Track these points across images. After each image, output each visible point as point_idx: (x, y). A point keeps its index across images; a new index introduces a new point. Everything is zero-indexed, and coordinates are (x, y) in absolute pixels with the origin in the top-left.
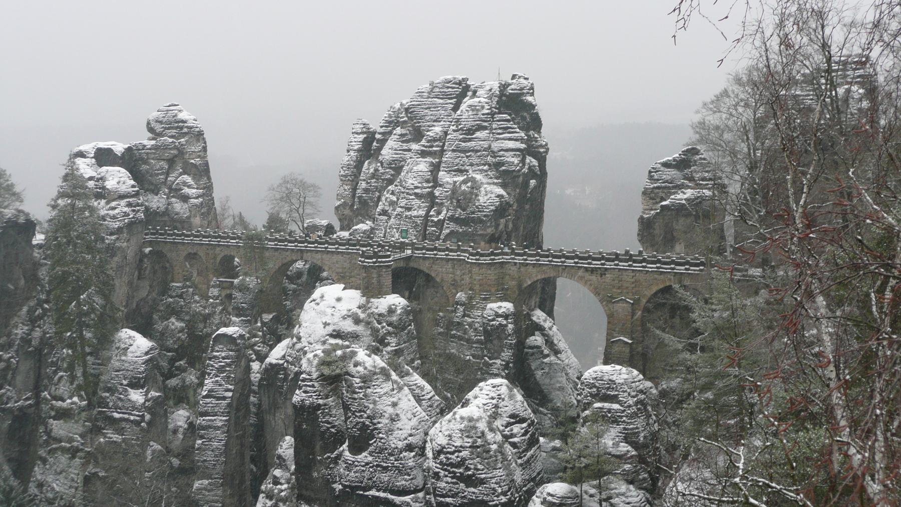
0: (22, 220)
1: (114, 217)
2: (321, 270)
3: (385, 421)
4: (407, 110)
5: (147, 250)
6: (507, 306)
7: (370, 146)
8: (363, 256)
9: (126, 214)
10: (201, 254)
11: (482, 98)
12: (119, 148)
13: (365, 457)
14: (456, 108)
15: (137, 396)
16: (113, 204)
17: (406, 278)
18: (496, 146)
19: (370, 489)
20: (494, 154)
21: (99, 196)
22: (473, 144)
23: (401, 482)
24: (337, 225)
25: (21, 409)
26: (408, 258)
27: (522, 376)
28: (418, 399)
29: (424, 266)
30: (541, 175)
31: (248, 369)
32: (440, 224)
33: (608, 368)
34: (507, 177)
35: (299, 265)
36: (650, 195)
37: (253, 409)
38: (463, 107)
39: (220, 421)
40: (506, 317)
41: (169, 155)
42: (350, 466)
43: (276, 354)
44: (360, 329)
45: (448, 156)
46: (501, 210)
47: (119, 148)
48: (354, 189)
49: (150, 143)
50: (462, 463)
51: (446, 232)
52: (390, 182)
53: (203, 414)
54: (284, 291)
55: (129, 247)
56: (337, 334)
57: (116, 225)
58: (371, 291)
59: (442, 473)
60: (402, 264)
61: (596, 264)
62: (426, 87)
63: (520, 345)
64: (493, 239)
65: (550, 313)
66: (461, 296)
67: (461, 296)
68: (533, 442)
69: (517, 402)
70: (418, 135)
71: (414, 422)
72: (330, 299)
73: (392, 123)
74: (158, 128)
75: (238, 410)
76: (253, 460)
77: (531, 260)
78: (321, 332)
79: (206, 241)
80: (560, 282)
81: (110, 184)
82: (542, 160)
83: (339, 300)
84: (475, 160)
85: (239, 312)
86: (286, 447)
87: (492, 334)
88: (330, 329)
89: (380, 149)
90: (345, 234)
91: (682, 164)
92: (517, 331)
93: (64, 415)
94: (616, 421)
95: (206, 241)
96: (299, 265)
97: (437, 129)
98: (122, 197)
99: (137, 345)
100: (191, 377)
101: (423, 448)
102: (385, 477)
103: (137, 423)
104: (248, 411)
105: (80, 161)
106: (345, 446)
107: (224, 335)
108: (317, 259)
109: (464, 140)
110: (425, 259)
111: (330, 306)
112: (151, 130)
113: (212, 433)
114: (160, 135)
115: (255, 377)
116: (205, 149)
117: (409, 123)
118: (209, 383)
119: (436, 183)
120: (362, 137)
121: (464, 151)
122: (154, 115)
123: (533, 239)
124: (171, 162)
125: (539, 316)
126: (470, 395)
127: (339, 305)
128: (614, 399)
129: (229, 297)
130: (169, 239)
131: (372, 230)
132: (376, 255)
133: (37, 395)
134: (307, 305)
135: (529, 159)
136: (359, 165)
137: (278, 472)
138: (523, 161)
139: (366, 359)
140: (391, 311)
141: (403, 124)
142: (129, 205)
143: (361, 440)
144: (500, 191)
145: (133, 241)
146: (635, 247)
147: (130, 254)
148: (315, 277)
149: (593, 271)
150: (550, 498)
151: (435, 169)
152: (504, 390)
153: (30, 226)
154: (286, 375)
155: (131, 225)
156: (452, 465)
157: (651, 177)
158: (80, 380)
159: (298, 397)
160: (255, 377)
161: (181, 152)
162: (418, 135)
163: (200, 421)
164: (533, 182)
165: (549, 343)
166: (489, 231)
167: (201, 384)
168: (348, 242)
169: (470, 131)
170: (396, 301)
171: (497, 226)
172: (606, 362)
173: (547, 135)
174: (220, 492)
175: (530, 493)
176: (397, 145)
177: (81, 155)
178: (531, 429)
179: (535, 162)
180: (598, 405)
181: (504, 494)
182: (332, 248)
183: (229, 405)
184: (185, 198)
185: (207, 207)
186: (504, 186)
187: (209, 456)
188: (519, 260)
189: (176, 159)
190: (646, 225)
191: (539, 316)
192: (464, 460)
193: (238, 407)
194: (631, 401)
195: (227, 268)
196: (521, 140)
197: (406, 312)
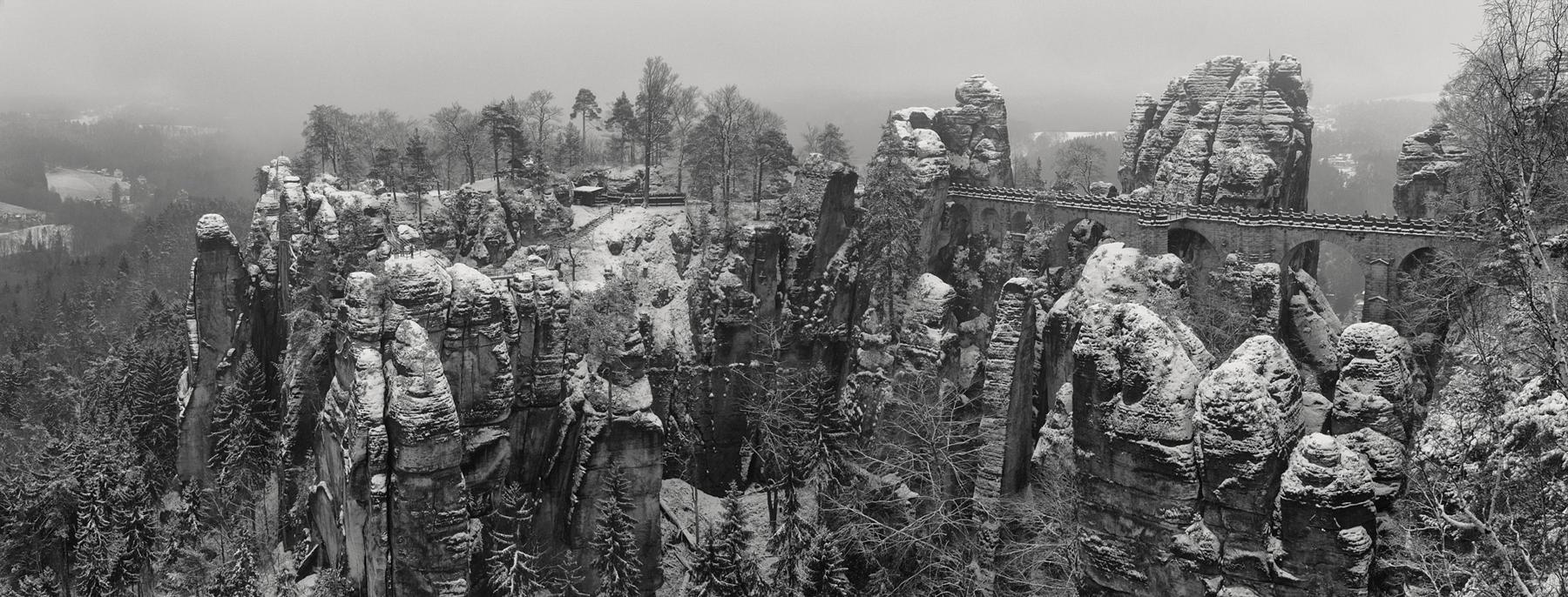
0: (846, 172)
1: (923, 173)
2: (1103, 228)
3: (1157, 373)
4: (1186, 85)
5: (950, 204)
6: (1274, 267)
7: (1152, 117)
8: (1142, 216)
9: (934, 171)
10: (998, 208)
11: (1254, 77)
12: (931, 113)
13: (1137, 407)
14: (1230, 85)
15: (936, 335)
16: (924, 161)
17: (1182, 239)
18: (1266, 119)
19: (1142, 438)
20: (1264, 127)
21: (912, 154)
22: (1244, 117)
23: (1173, 433)
24: (1119, 188)
25: (837, 336)
26: (1185, 220)
27: (1288, 332)
28: (1190, 354)
29: (1198, 228)
30: (1307, 149)
31: (1034, 318)
32: (1213, 190)
33: (1367, 325)
34: (1273, 146)
35: (1084, 223)
36: (1405, 166)
37: (1038, 355)
38: (1237, 84)
39: (1007, 363)
40: (1273, 277)
41: (971, 122)
42: (1125, 416)
43: (1061, 305)
44: (1137, 285)
45: (1222, 127)
46: (1269, 179)
47: (931, 113)
48: (1136, 156)
49: (957, 110)
50: (1229, 416)
51: (1219, 196)
52: (1169, 150)
53: (993, 356)
54: (1070, 247)
55: (935, 201)
56: (1116, 290)
57: (925, 180)
58: (1149, 250)
59: (1210, 425)
60: (1177, 226)
61: (1356, 228)
62: (1202, 65)
63: (1286, 303)
64: (1263, 205)
65: (1313, 275)
66: (1232, 257)
67: (1232, 257)
68: (1296, 396)
69: (1283, 358)
70: (1194, 108)
71: (1185, 375)
72: (1110, 257)
73: (1172, 96)
74: (965, 96)
75: (1023, 354)
76: (1035, 402)
77: (1296, 224)
78: (1102, 286)
79: (1001, 198)
80: (1323, 245)
81: (922, 144)
82: (1307, 133)
83: (1119, 257)
84: (1246, 132)
85: (1027, 264)
86: (1065, 392)
87: (1261, 295)
88: (1109, 284)
89: (1160, 120)
90: (1125, 197)
91: (1432, 139)
92: (1284, 291)
93: (871, 346)
94: (1373, 376)
95: (1001, 198)
96: (1084, 223)
97: (1212, 104)
98: (931, 156)
99: (935, 287)
100: (983, 321)
101: (1193, 401)
102: (1156, 427)
103: (933, 360)
104: (1033, 357)
105: (898, 124)
106: (1119, 395)
107: (1014, 285)
108: (1101, 218)
109: (1238, 114)
110: (1198, 221)
111: (1113, 259)
112: (959, 97)
113: (1000, 375)
114: (967, 102)
115: (1040, 325)
116: (1004, 116)
117: (1187, 97)
118: (999, 327)
119: (1211, 153)
120: (1144, 109)
121: (1237, 123)
122: (961, 85)
123: (1299, 204)
124: (975, 126)
125: (1302, 276)
126: (1236, 351)
127: (1118, 263)
128: (1372, 355)
129: (1021, 250)
130: (970, 195)
131: (1151, 194)
132: (1154, 217)
133: (850, 327)
134: (1090, 261)
135: (1296, 132)
136: (1141, 135)
137: (1056, 417)
138: (1290, 133)
139: (1144, 316)
140: (1166, 271)
141: (1182, 98)
142: (937, 163)
143: (1136, 389)
144: (1269, 161)
145: (939, 195)
146: (1390, 212)
147: (936, 207)
148: (1098, 234)
149: (1353, 234)
150: (1311, 451)
151: (1210, 140)
152: (1269, 347)
153: (853, 178)
154: (1069, 325)
155: (937, 181)
156: (1220, 418)
157: (1405, 151)
158: (887, 318)
159: (1078, 347)
160: (1040, 325)
161: (984, 119)
162: (1194, 108)
163: (989, 362)
164: (1299, 153)
165: (1313, 302)
166: (1259, 197)
167: (992, 327)
168: (1128, 204)
169: (1243, 106)
170: (1172, 260)
171: (1266, 192)
172: (1363, 321)
173: (1312, 110)
174: (1004, 431)
175: (1293, 444)
176: (1176, 117)
177: (899, 118)
178: (1295, 384)
179: (1301, 135)
180: (1356, 360)
181: (1268, 446)
182: (1114, 209)
183: (1016, 350)
184: (985, 159)
185: (1004, 167)
186: (1272, 156)
187: (996, 396)
188: (1286, 224)
189: (980, 124)
190: (1401, 193)
191: (1302, 276)
192: (1231, 414)
193: (1024, 351)
194: (1387, 357)
195: (1020, 224)
196: (1289, 114)
197: (1181, 271)
